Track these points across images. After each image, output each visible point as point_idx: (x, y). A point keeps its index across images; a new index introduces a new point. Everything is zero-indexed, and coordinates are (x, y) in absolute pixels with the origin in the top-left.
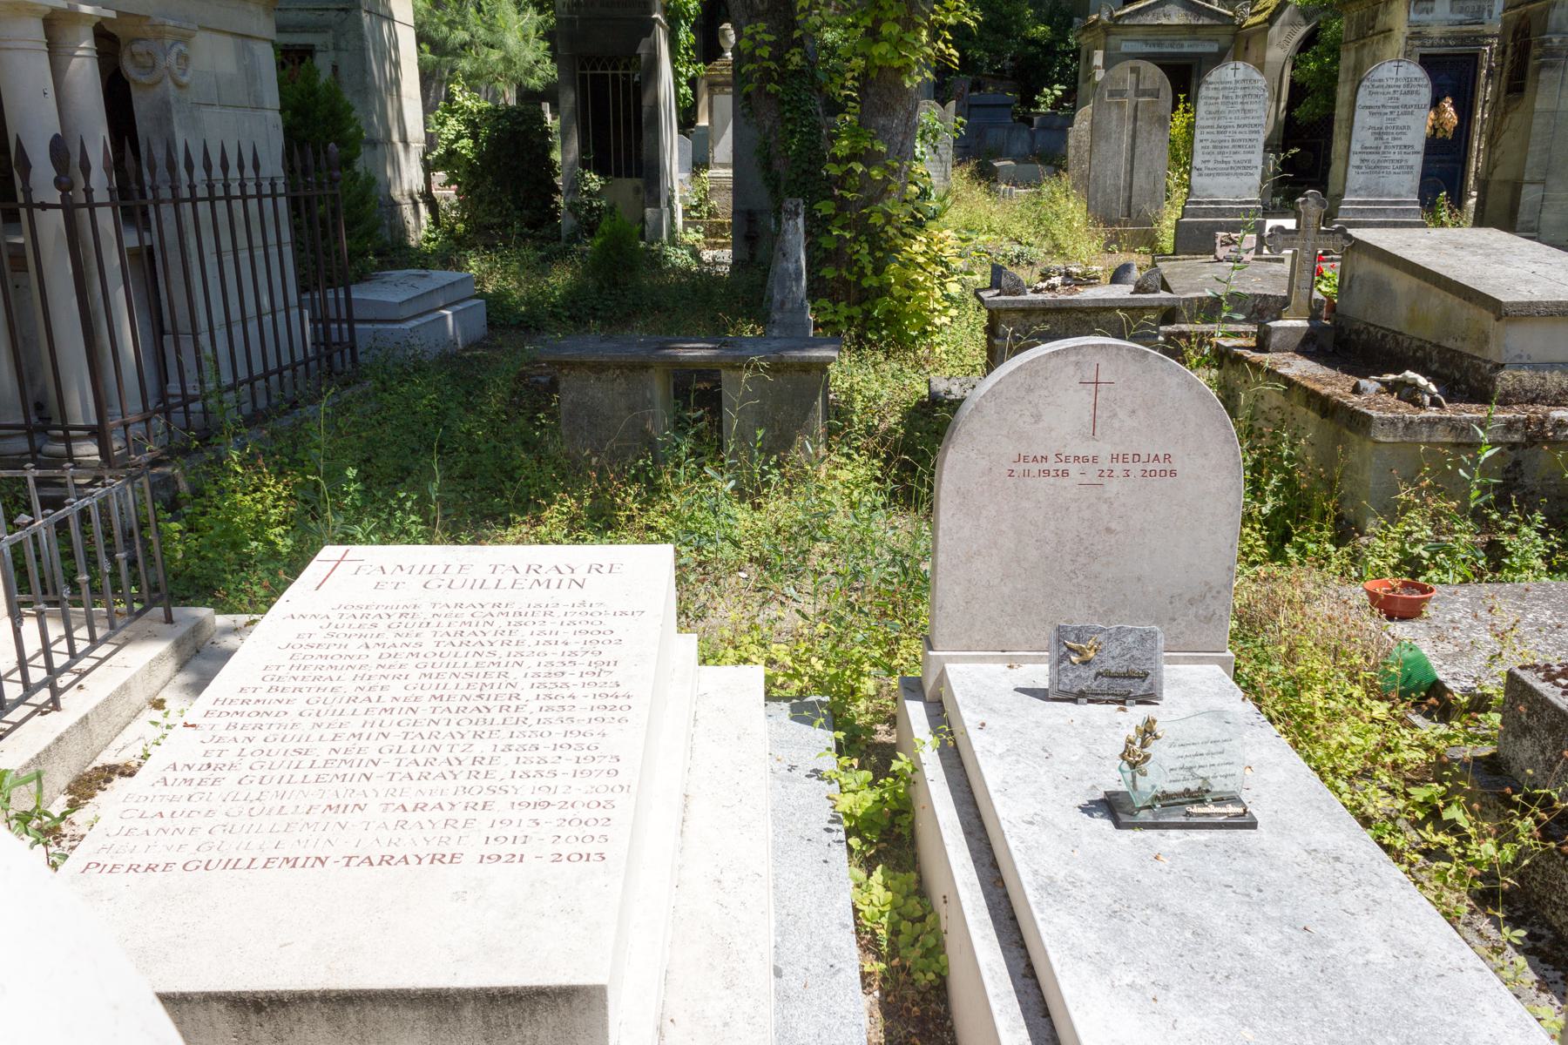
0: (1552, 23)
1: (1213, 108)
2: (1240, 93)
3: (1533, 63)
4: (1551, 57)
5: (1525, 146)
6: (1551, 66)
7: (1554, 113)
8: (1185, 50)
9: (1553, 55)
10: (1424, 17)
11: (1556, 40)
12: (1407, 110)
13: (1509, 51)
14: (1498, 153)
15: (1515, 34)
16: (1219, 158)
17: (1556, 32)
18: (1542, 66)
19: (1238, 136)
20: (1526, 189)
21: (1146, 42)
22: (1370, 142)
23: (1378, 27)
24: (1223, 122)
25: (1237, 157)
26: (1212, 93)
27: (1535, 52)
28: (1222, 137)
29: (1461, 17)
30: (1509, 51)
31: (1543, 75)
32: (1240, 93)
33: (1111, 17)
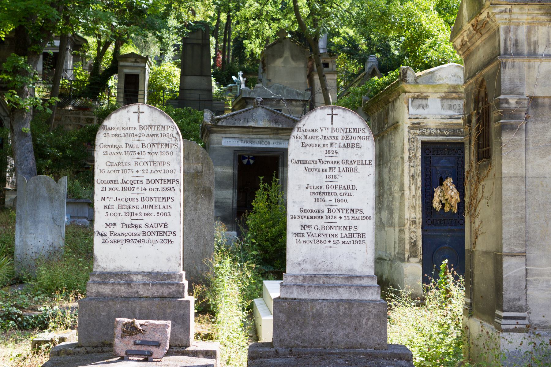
0: (506, 83)
1: (115, 159)
2: (147, 141)
3: (494, 126)
4: (512, 120)
5: (499, 214)
6: (512, 128)
7: (523, 178)
8: (271, 146)
9: (512, 117)
10: (420, 112)
11: (513, 101)
12: (350, 167)
13: (474, 120)
14: (477, 221)
15: (476, 102)
16: (128, 220)
17: (511, 93)
18: (502, 128)
19: (148, 194)
20: (507, 262)
21: (241, 139)
22: (310, 203)
23: (390, 121)
24: (128, 177)
25: (149, 220)
26: (112, 141)
27: (494, 115)
28: (128, 194)
29: (451, 113)
30: (474, 120)
31: (506, 138)
32: (147, 141)
33: (212, 120)
